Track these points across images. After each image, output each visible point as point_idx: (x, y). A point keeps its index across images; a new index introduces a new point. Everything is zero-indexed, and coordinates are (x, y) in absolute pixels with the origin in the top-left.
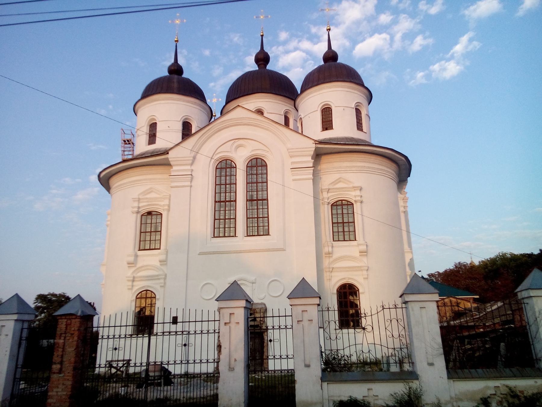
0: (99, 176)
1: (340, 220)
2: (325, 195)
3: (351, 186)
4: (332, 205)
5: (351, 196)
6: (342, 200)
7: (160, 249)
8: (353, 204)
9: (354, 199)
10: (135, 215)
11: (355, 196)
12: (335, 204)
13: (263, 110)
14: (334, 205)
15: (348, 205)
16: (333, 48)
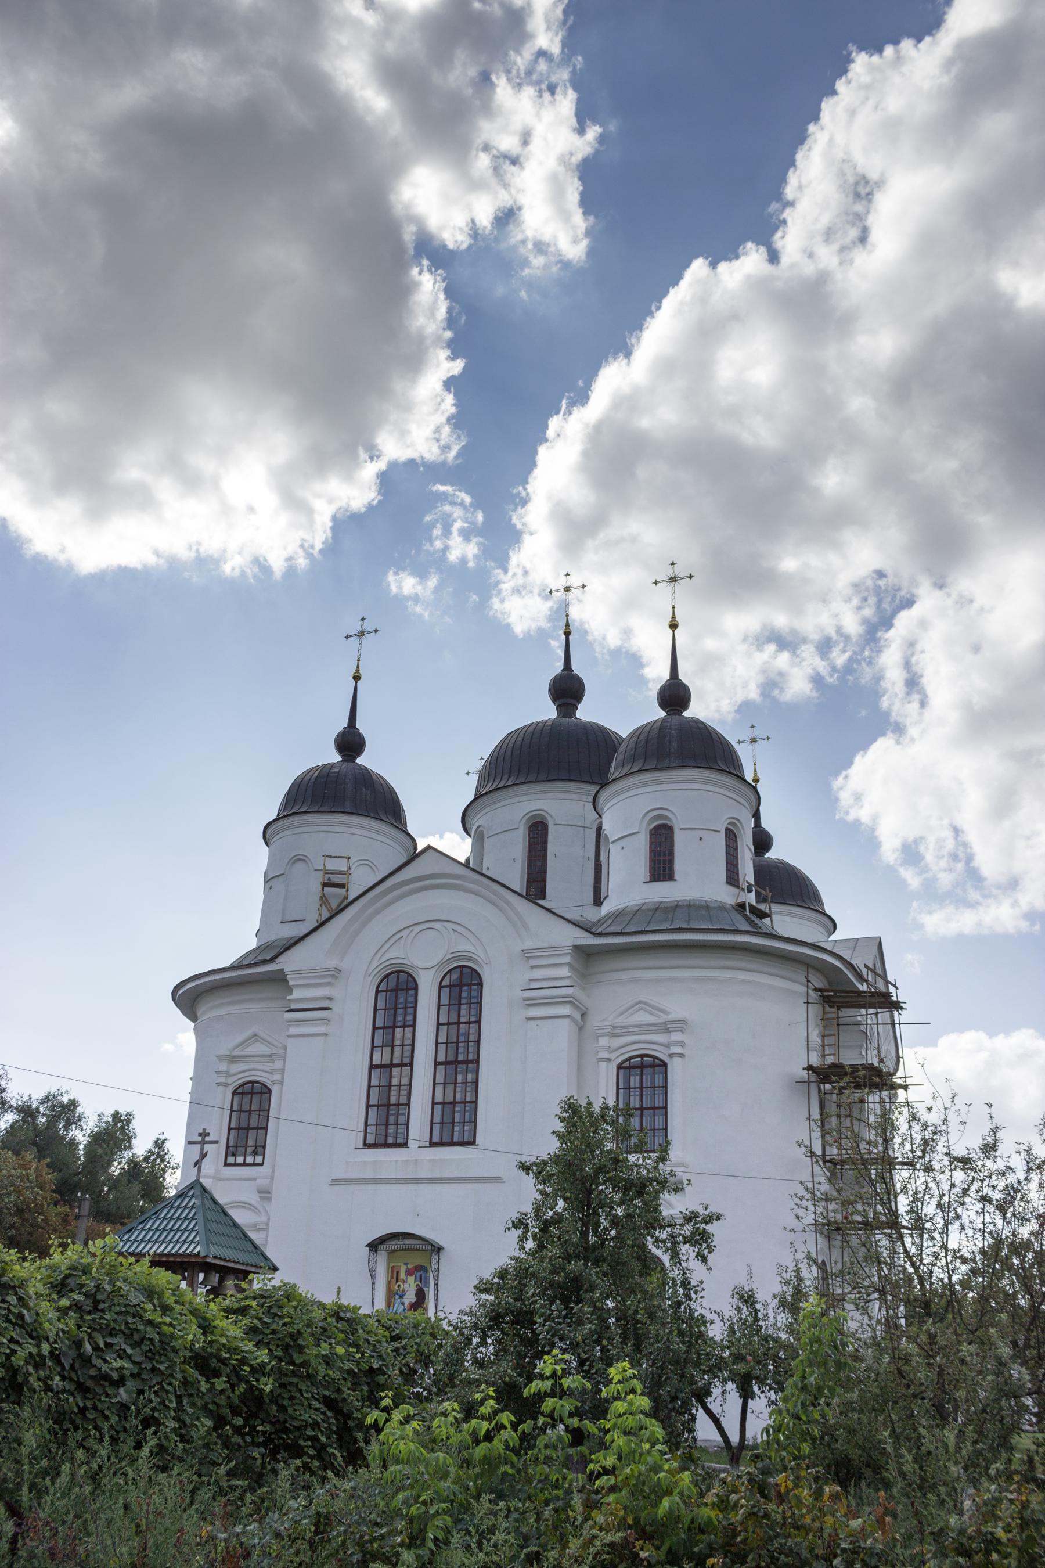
0: (173, 999)
1: (635, 1102)
2: (603, 1042)
3: (664, 1018)
4: (619, 1067)
5: (654, 1044)
6: (642, 1056)
7: (261, 1165)
8: (664, 1065)
9: (667, 1052)
10: (221, 1088)
11: (667, 1046)
12: (627, 1064)
13: (545, 818)
14: (625, 1068)
15: (653, 1066)
16: (682, 676)
